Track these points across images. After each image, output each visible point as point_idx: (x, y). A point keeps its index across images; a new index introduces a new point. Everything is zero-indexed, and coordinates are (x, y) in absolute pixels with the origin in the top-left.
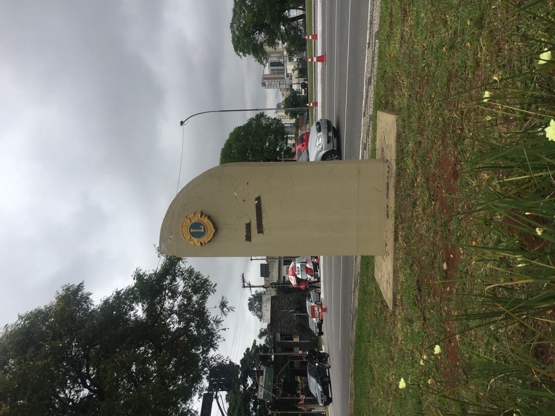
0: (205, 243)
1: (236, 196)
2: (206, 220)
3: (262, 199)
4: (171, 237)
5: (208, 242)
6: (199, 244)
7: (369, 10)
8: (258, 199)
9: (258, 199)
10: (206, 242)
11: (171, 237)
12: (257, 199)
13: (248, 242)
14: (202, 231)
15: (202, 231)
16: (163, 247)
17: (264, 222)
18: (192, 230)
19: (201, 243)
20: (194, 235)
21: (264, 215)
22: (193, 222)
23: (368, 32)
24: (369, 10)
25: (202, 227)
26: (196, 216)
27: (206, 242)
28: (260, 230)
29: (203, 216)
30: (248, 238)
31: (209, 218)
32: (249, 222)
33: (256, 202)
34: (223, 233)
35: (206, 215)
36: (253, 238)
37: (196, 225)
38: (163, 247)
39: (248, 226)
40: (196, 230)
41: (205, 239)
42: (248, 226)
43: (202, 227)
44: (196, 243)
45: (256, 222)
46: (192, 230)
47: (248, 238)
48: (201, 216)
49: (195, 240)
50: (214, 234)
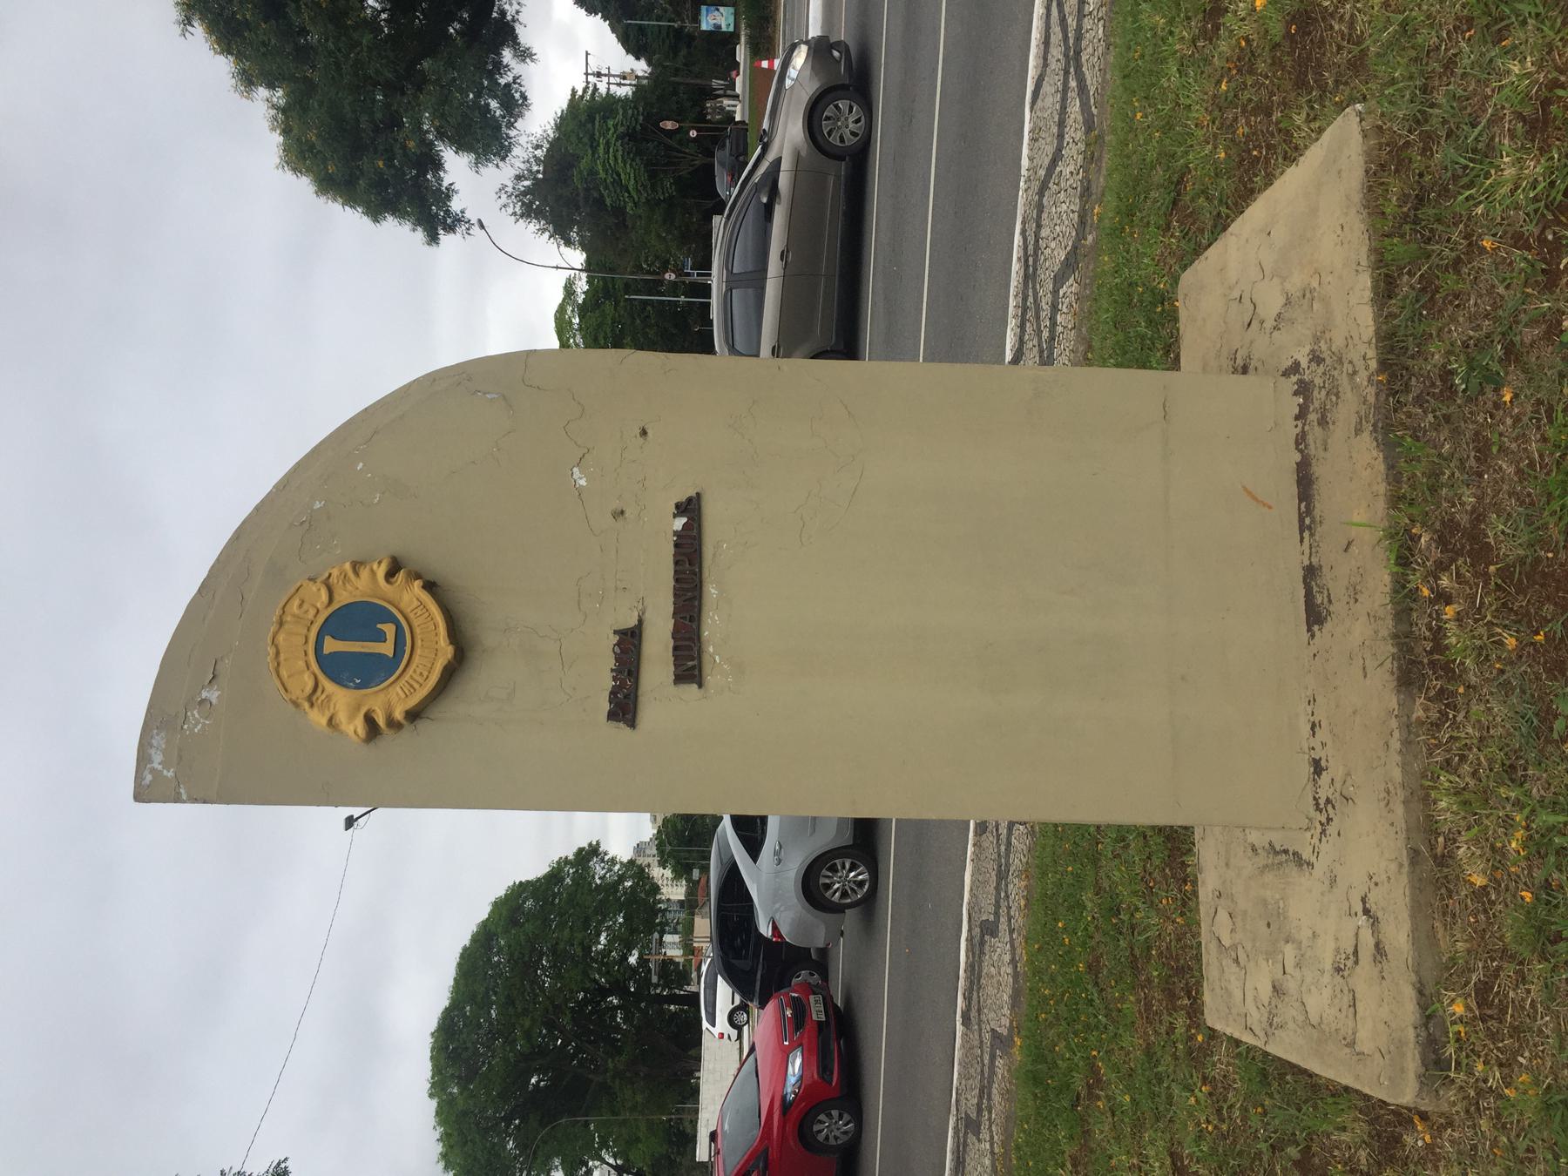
0: (393, 724)
1: (580, 491)
2: (411, 597)
3: (712, 514)
4: (213, 695)
5: (414, 715)
6: (359, 725)
7: (1016, 253)
8: (690, 508)
9: (690, 508)
10: (398, 715)
11: (213, 695)
12: (683, 508)
13: (622, 730)
14: (387, 649)
15: (387, 649)
16: (157, 758)
17: (713, 625)
18: (331, 645)
19: (370, 721)
20: (337, 669)
21: (711, 591)
22: (343, 598)
23: (1012, 323)
24: (1016, 253)
25: (389, 629)
26: (365, 573)
27: (398, 715)
28: (689, 667)
29: (401, 575)
30: (624, 708)
31: (430, 586)
32: (633, 622)
33: (679, 523)
34: (490, 677)
35: (418, 576)
36: (650, 711)
37: (357, 619)
38: (157, 758)
39: (630, 642)
40: (354, 644)
41: (396, 697)
42: (630, 642)
43: (389, 629)
44: (342, 717)
45: (670, 625)
46: (331, 645)
47: (624, 708)
48: (390, 575)
49: (340, 698)
50: (450, 674)
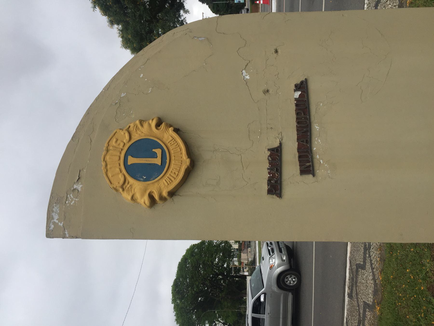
0: (162, 198)
1: (246, 81)
2: (168, 136)
3: (313, 87)
4: (79, 187)
5: (172, 194)
6: (146, 198)
8: (302, 86)
9: (302, 86)
10: (165, 194)
11: (79, 187)
14: (158, 161)
15: (158, 161)
16: (56, 217)
17: (318, 144)
18: (131, 160)
19: (151, 197)
20: (134, 171)
21: (316, 127)
22: (136, 137)
25: (158, 152)
26: (146, 125)
27: (165, 194)
28: (307, 166)
30: (275, 187)
31: (177, 130)
32: (276, 144)
33: (297, 94)
34: (206, 175)
35: (171, 126)
36: (288, 189)
38: (56, 217)
39: (276, 154)
40: (143, 161)
41: (162, 185)
42: (276, 154)
43: (158, 152)
44: (138, 196)
46: (131, 160)
47: (275, 187)
48: (158, 125)
49: (137, 186)
50: (189, 172)
